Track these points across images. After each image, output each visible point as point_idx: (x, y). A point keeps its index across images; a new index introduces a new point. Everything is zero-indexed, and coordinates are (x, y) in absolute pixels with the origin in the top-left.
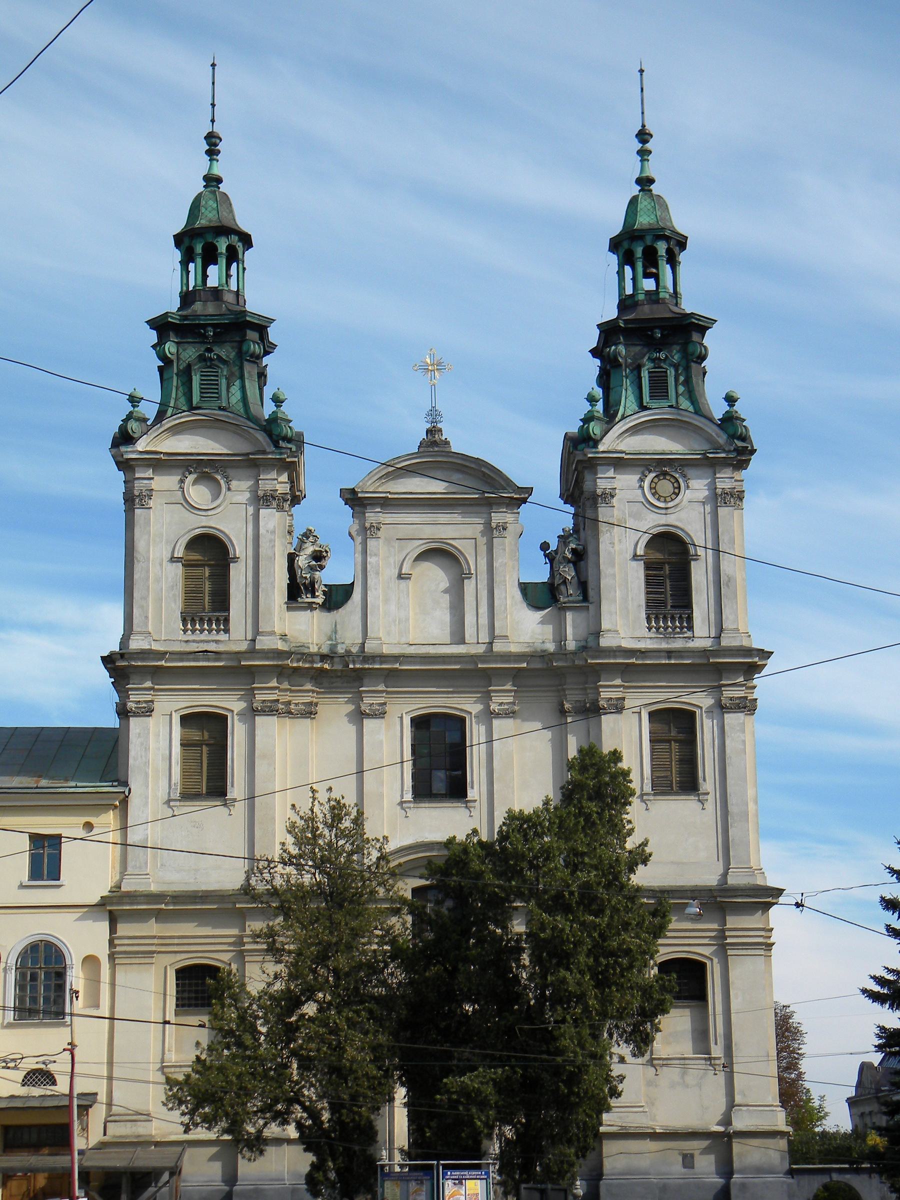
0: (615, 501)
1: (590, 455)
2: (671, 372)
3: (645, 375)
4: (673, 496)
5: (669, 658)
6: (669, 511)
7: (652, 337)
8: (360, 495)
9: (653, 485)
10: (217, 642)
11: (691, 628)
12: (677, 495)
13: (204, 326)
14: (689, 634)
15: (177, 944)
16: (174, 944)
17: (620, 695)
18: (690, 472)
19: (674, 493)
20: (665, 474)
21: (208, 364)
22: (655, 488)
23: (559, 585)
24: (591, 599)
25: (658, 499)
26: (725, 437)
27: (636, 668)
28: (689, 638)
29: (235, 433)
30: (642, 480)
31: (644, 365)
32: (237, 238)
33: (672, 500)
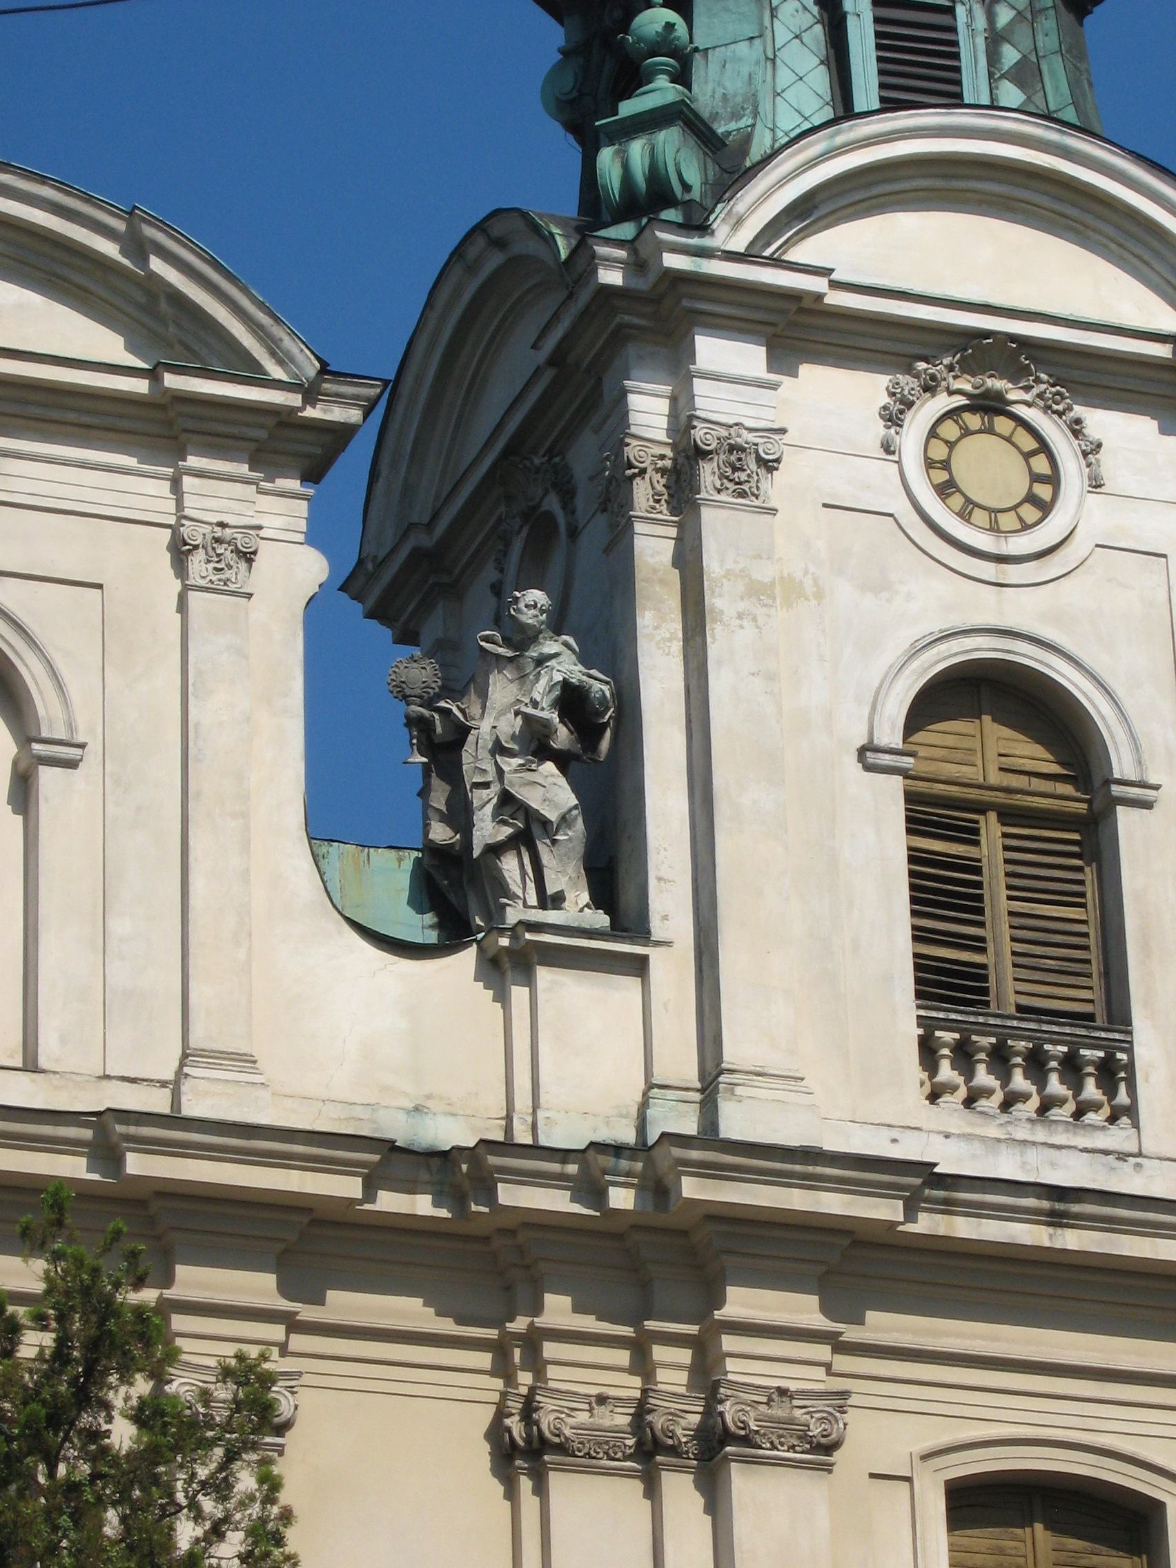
0: (775, 488)
1: (672, 261)
4: (1030, 514)
5: (1056, 1219)
6: (1013, 573)
11: (1125, 1113)
12: (1045, 508)
14: (1119, 1137)
17: (814, 1380)
19: (1031, 499)
20: (989, 405)
22: (946, 465)
23: (495, 850)
24: (658, 929)
25: (964, 515)
27: (884, 1257)
28: (1122, 1156)
30: (893, 419)
33: (1025, 527)
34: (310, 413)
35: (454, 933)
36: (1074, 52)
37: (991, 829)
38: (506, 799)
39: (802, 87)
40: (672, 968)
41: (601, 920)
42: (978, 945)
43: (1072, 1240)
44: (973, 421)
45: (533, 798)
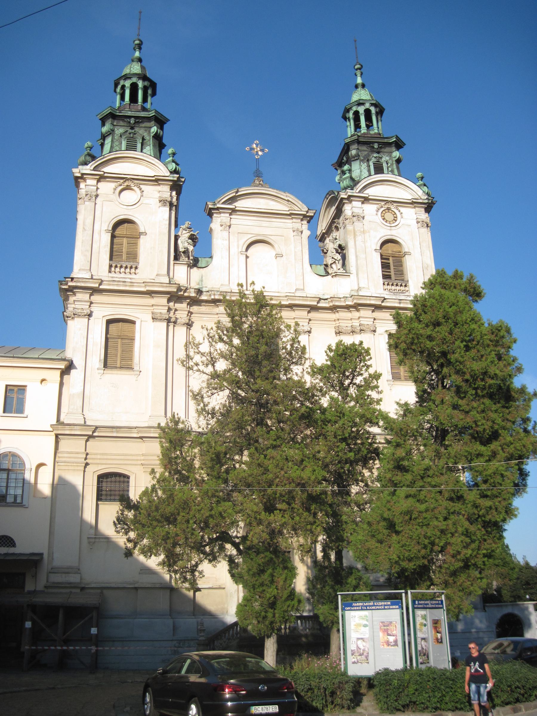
2: (385, 165)
3: (371, 164)
4: (394, 221)
7: (373, 147)
8: (219, 206)
9: (383, 215)
10: (130, 278)
12: (396, 221)
13: (130, 117)
15: (100, 459)
16: (97, 459)
18: (402, 209)
19: (394, 220)
21: (132, 136)
25: (386, 222)
26: (421, 192)
29: (147, 166)
31: (371, 160)
32: (149, 84)
34: (308, 214)
35: (327, 274)
36: (398, 168)
37: (391, 258)
38: (333, 258)
39: (365, 173)
40: (353, 277)
41: (345, 271)
42: (390, 272)
43: (402, 305)
44: (387, 211)
45: (336, 258)
